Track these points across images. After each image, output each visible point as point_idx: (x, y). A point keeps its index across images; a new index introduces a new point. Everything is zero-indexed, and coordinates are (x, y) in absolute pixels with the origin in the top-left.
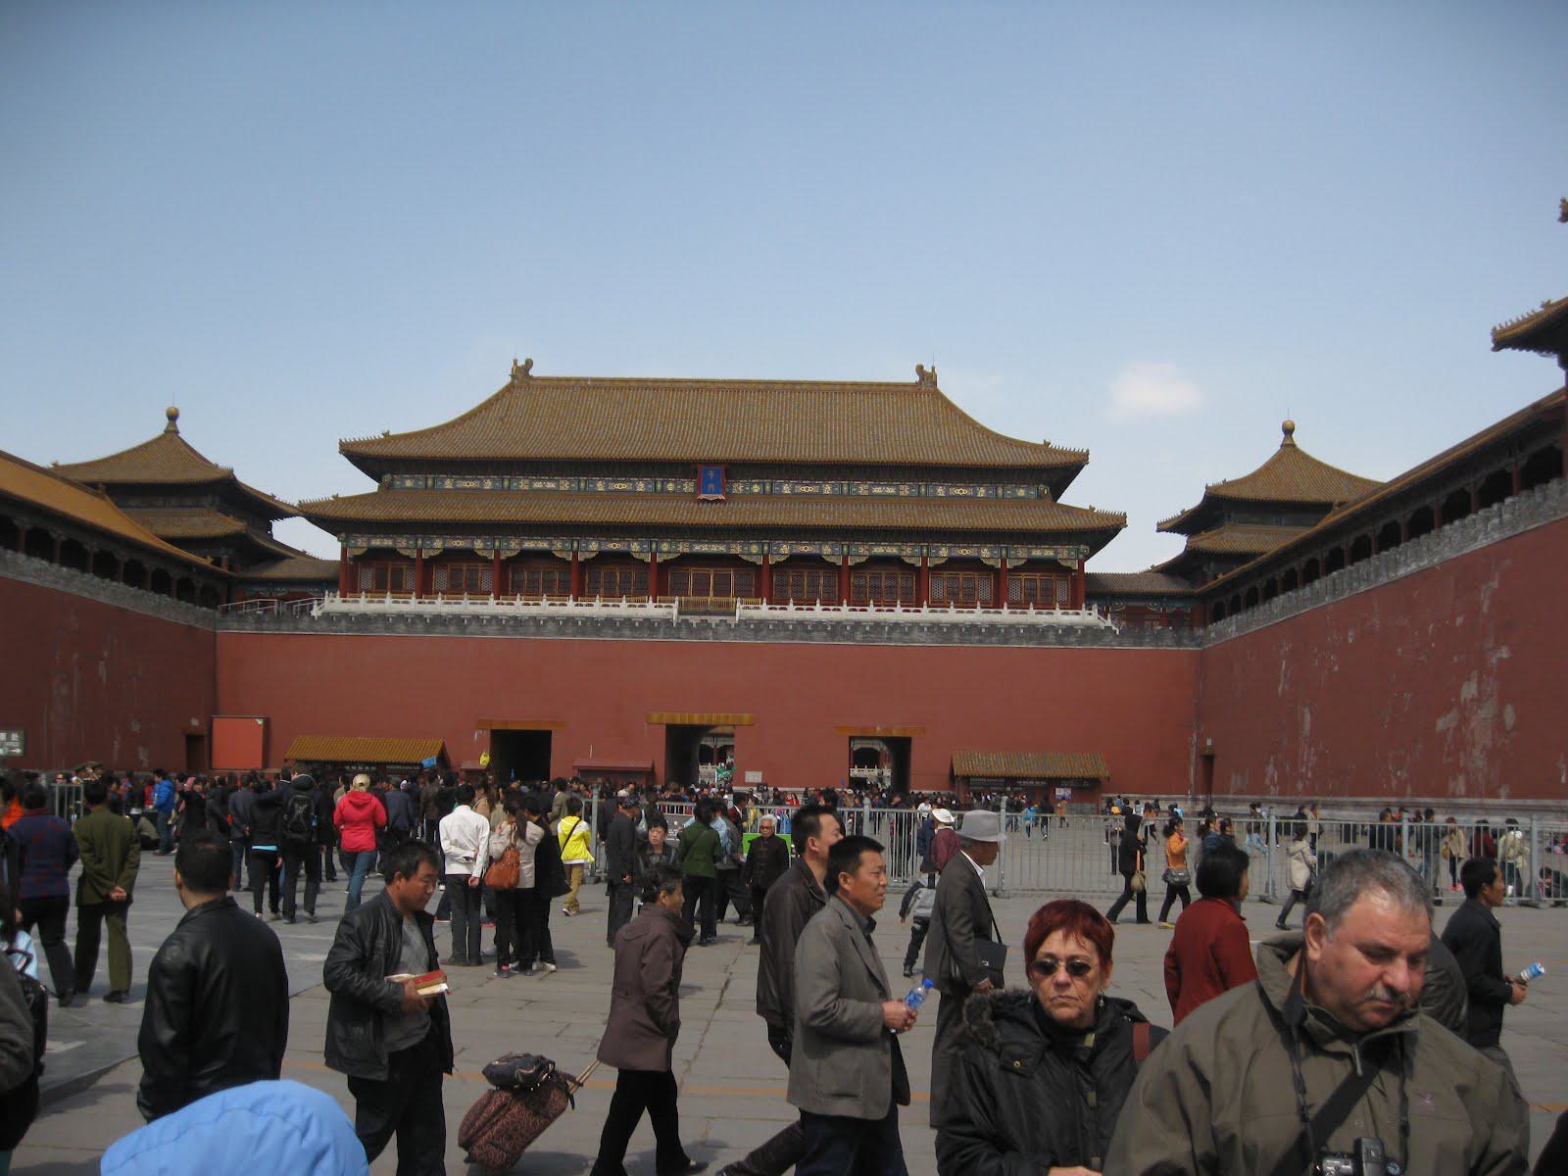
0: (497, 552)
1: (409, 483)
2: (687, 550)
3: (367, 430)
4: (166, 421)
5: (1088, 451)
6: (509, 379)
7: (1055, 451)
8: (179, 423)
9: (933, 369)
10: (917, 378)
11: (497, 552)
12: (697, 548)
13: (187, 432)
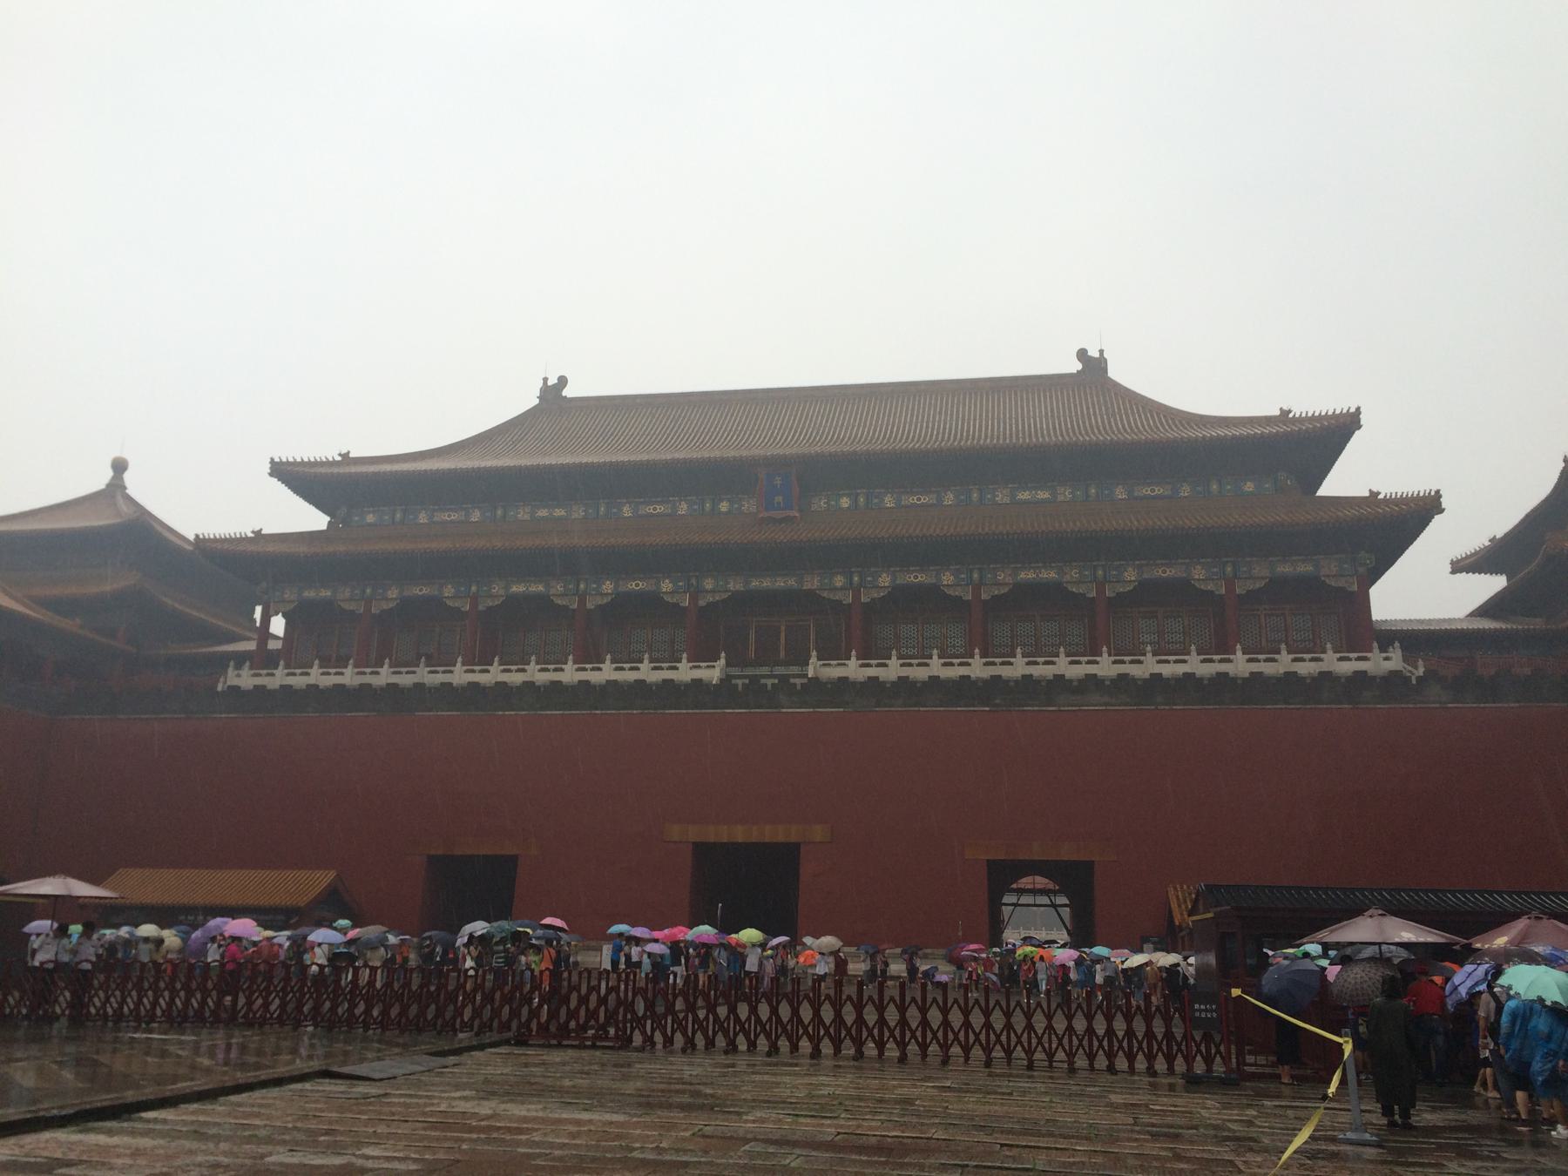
0: (475, 600)
2: (740, 587)
3: (318, 445)
4: (109, 474)
5: (1358, 409)
6: (537, 401)
7: (1295, 420)
8: (128, 477)
9: (1101, 352)
10: (1079, 366)
11: (475, 600)
12: (755, 583)
13: (137, 486)
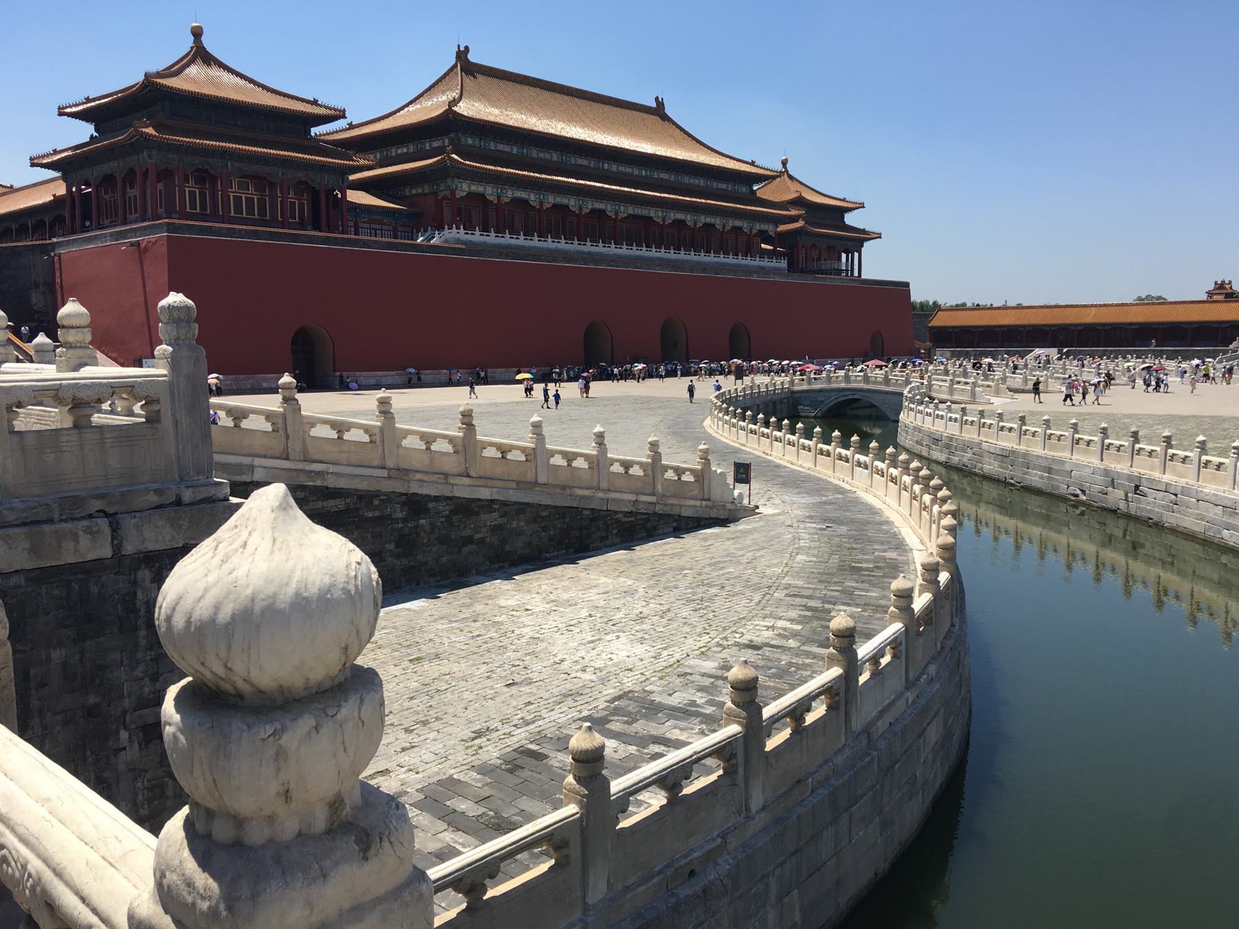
1: (470, 141)
8: (203, 39)
10: (654, 105)
